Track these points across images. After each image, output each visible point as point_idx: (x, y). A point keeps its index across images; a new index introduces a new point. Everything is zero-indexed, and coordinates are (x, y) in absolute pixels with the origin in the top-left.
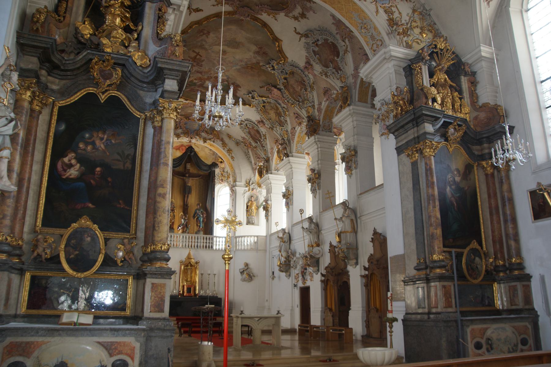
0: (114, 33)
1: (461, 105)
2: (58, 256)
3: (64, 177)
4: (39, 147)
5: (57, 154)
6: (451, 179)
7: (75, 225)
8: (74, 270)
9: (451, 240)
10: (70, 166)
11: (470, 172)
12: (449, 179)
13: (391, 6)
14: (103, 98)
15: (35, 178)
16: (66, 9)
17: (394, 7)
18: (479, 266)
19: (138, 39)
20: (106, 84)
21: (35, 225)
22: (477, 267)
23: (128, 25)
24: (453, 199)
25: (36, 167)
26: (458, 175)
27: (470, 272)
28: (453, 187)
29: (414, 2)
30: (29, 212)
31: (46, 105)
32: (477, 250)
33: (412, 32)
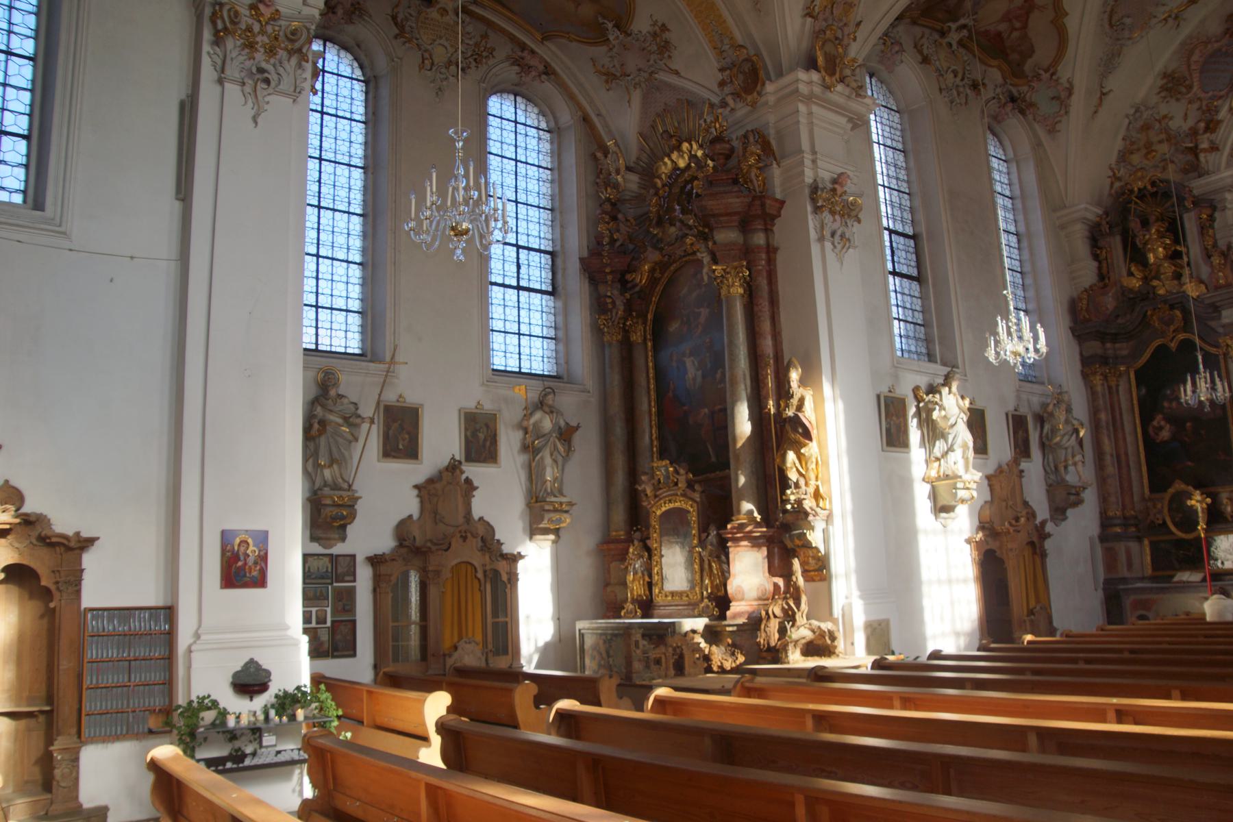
0: (1162, 270)
2: (1164, 523)
3: (1158, 441)
4: (1127, 418)
5: (1146, 419)
7: (1171, 491)
8: (1186, 532)
10: (1161, 428)
14: (1173, 345)
15: (1131, 449)
16: (1108, 267)
19: (1189, 264)
20: (1171, 330)
21: (1143, 494)
23: (1176, 250)
25: (1129, 439)
30: (1135, 484)
31: (1120, 375)
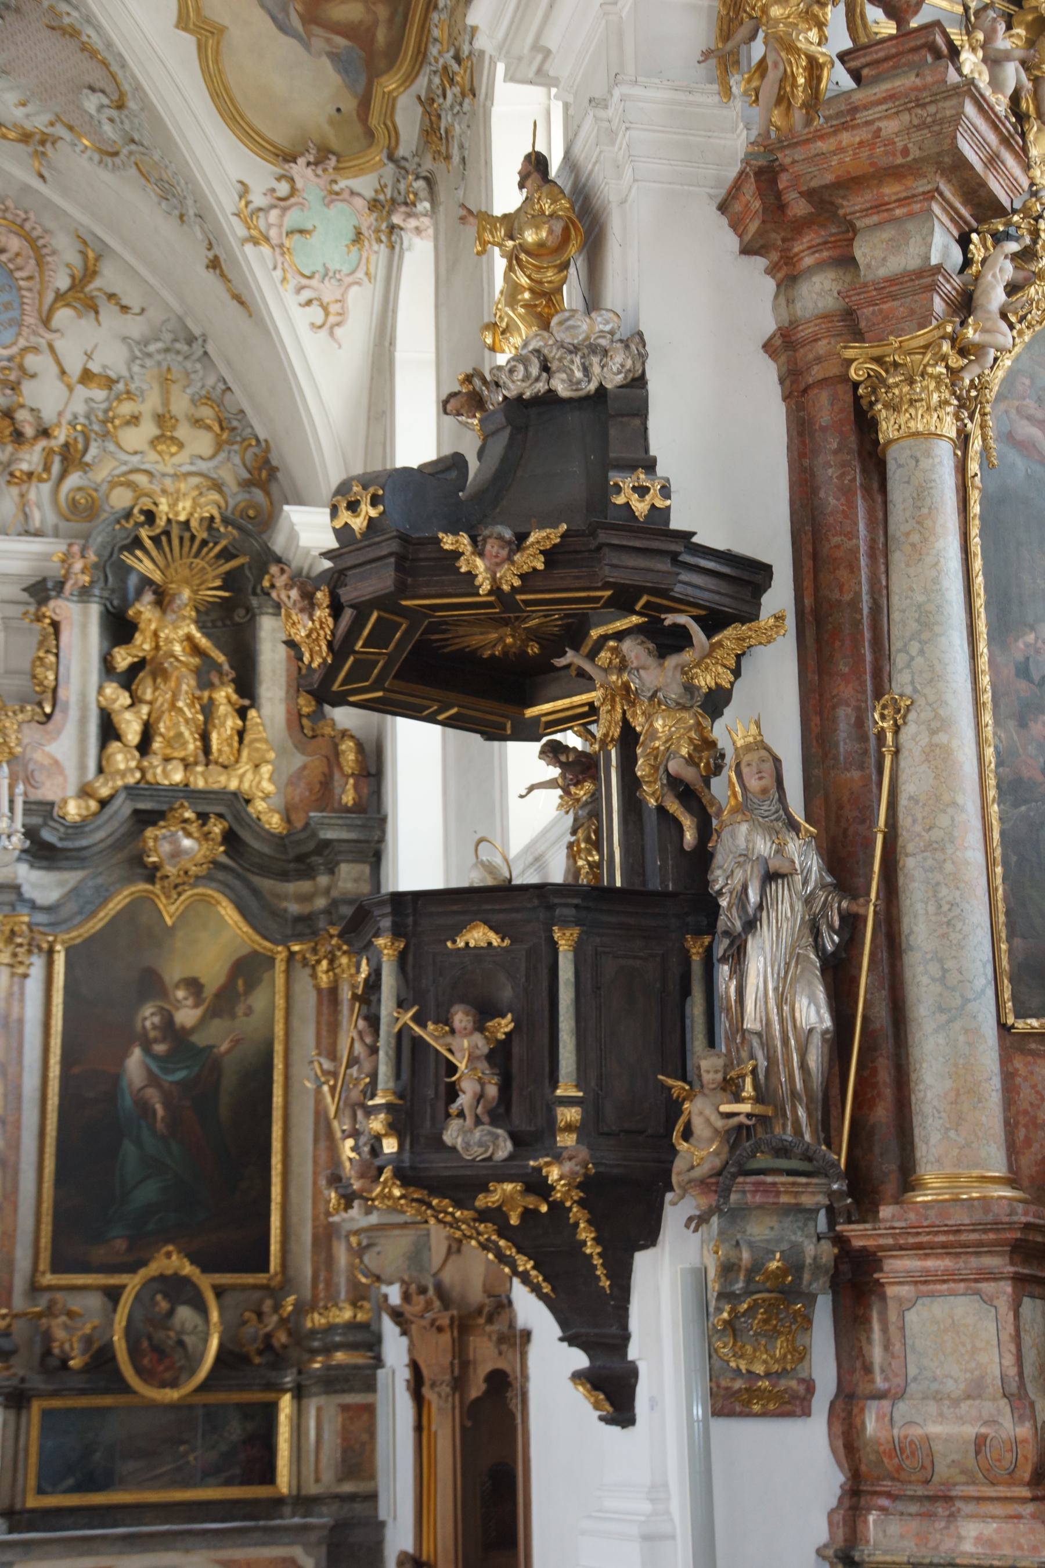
1: (241, 734)
6: (156, 1020)
9: (121, 1245)
11: (251, 986)
12: (145, 1019)
13: (25, 350)
17: (35, 349)
18: (189, 1340)
22: (181, 1343)
24: (153, 1095)
26: (190, 1002)
27: (146, 1361)
28: (160, 1048)
29: (143, 310)
32: (186, 1281)
33: (111, 447)
